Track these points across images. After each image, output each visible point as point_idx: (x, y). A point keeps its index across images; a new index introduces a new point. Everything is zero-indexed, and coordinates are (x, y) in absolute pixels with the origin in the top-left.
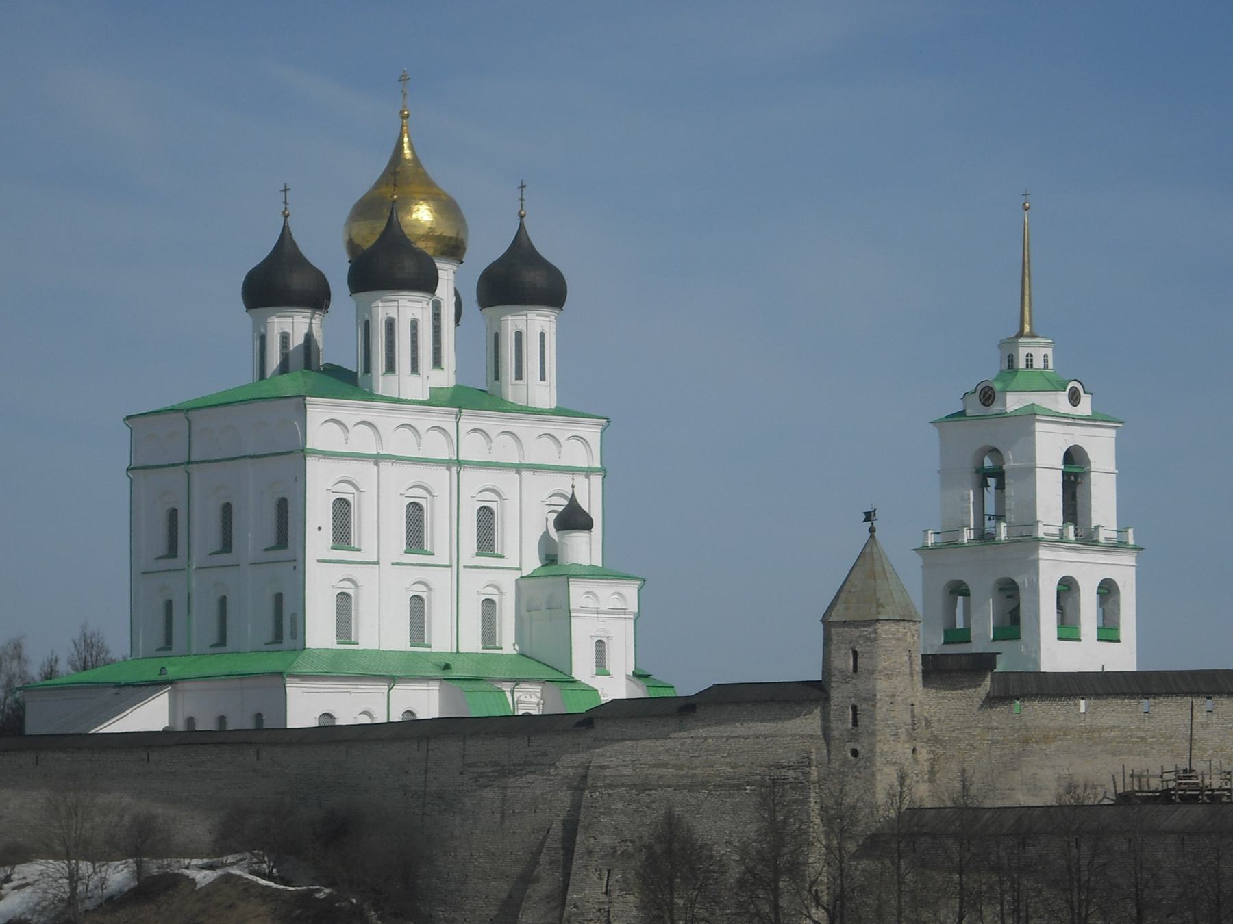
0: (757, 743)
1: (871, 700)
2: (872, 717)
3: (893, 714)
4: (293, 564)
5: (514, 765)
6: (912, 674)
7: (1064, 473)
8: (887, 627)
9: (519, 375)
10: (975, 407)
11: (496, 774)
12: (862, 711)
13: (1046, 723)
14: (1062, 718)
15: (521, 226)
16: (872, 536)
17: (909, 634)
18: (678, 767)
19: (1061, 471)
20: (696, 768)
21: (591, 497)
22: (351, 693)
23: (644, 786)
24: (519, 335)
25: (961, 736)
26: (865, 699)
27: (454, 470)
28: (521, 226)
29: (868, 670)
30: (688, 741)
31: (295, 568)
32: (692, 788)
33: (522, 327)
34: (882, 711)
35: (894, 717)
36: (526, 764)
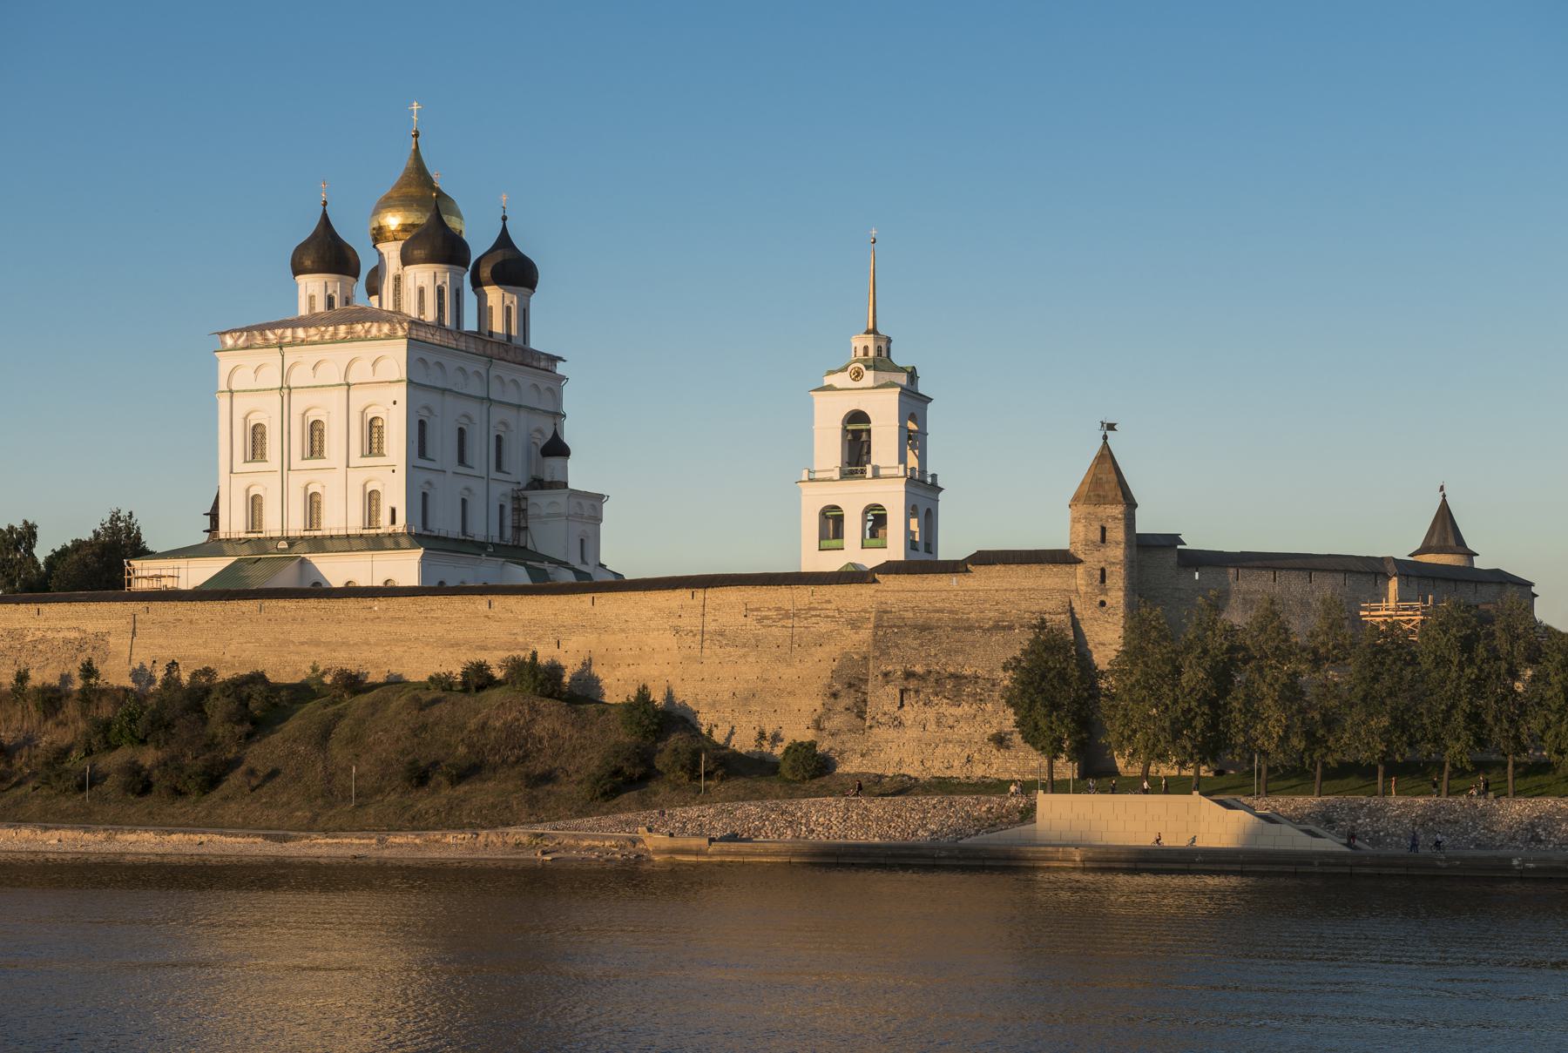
0: (1022, 595)
1: (1118, 564)
4: (394, 468)
5: (799, 610)
11: (781, 617)
15: (504, 227)
16: (1105, 443)
18: (951, 612)
22: (455, 567)
23: (925, 628)
25: (1157, 595)
26: (1114, 563)
27: (485, 406)
28: (504, 227)
30: (962, 593)
31: (394, 471)
32: (969, 629)
36: (810, 609)
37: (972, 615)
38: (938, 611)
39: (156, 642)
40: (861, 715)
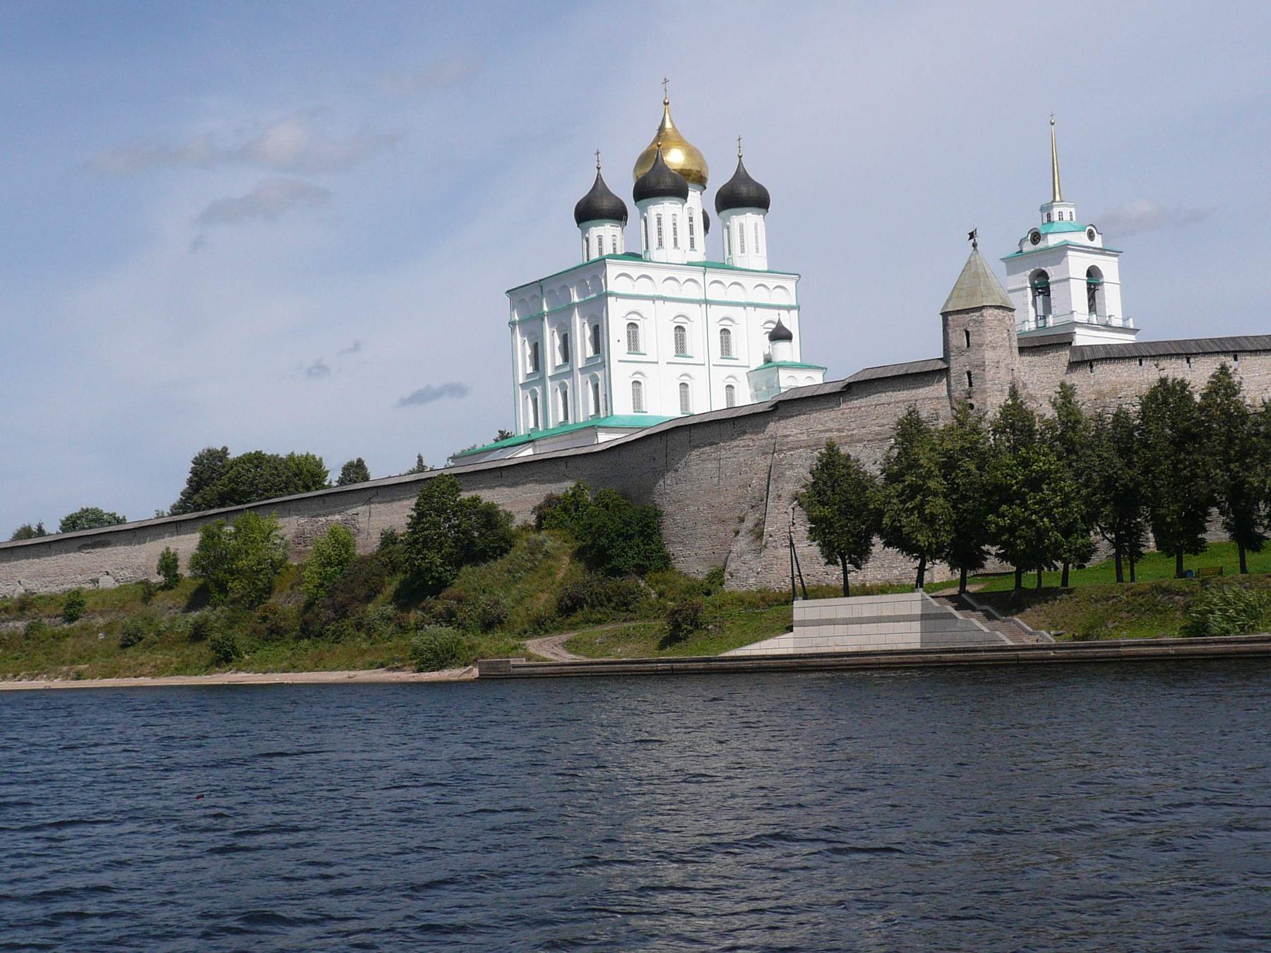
2: (984, 380)
3: (999, 375)
6: (1011, 347)
7: (1088, 283)
8: (990, 311)
9: (743, 251)
10: (1028, 247)
12: (975, 374)
13: (1114, 379)
14: (1126, 374)
17: (1007, 318)
18: (839, 430)
19: (1085, 282)
20: (853, 430)
21: (791, 322)
24: (741, 226)
29: (978, 344)
30: (846, 411)
33: (743, 222)
34: (990, 373)
35: (999, 378)
37: (854, 432)
38: (826, 431)
39: (382, 518)
40: (760, 535)
